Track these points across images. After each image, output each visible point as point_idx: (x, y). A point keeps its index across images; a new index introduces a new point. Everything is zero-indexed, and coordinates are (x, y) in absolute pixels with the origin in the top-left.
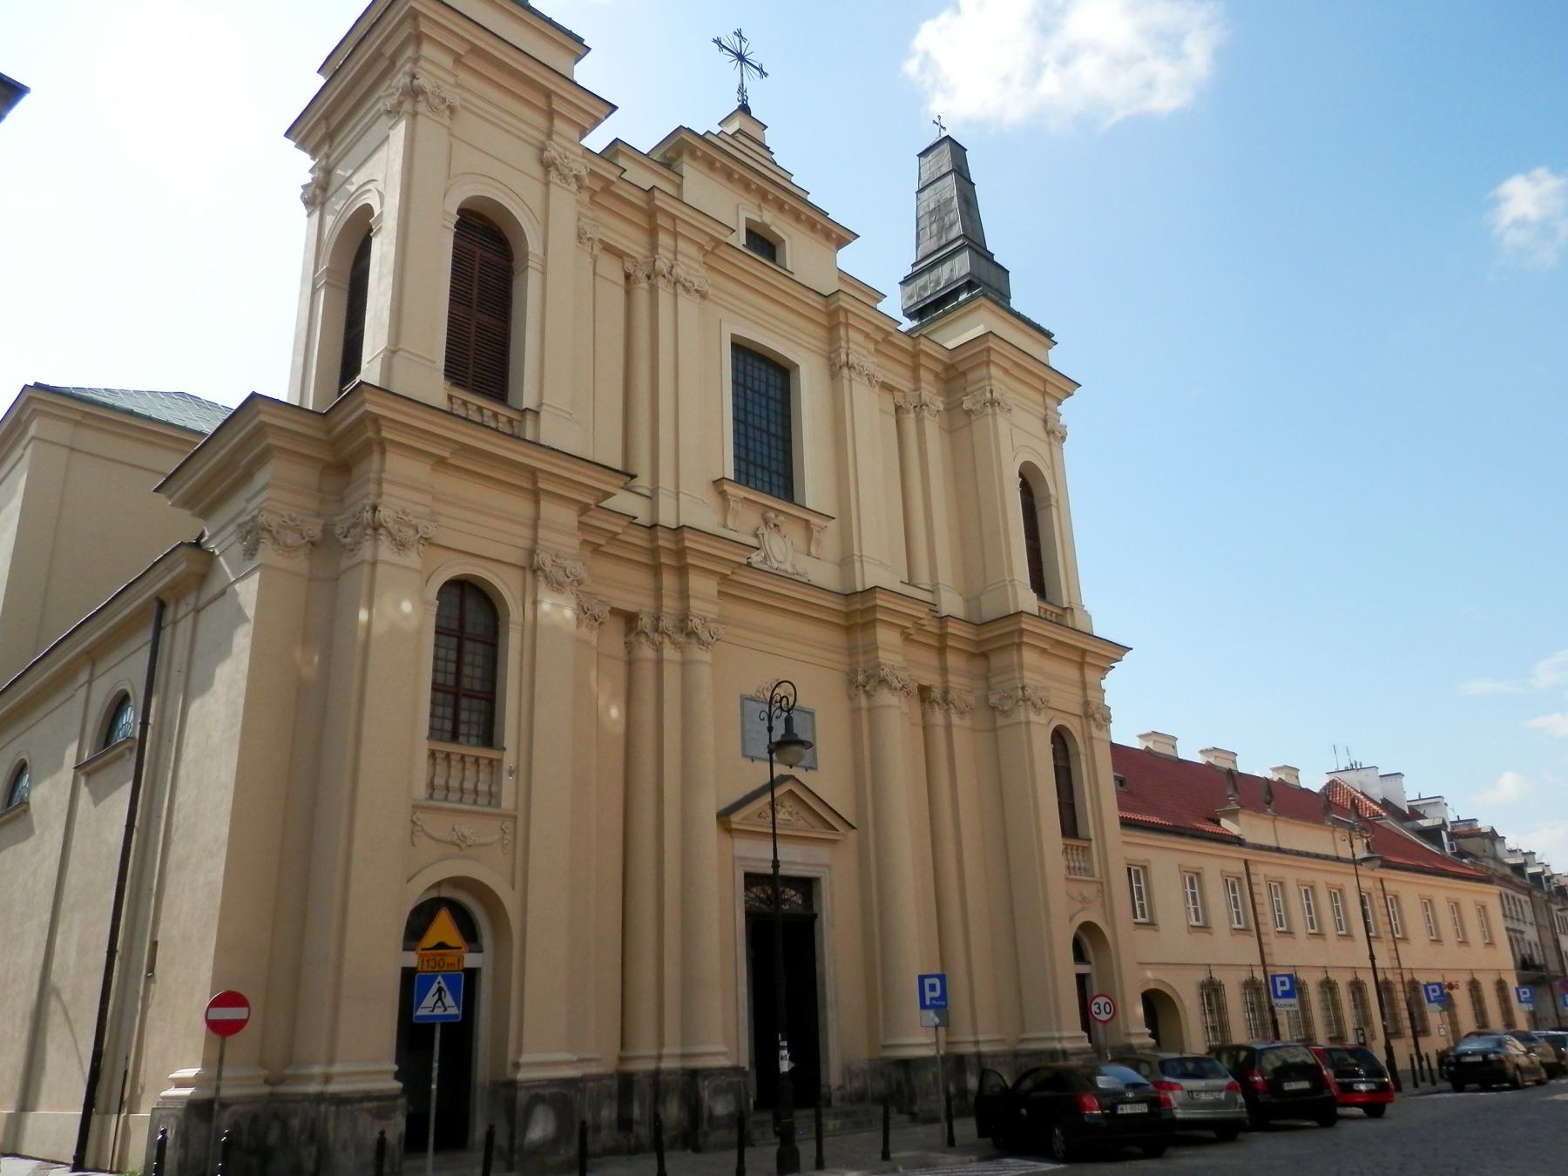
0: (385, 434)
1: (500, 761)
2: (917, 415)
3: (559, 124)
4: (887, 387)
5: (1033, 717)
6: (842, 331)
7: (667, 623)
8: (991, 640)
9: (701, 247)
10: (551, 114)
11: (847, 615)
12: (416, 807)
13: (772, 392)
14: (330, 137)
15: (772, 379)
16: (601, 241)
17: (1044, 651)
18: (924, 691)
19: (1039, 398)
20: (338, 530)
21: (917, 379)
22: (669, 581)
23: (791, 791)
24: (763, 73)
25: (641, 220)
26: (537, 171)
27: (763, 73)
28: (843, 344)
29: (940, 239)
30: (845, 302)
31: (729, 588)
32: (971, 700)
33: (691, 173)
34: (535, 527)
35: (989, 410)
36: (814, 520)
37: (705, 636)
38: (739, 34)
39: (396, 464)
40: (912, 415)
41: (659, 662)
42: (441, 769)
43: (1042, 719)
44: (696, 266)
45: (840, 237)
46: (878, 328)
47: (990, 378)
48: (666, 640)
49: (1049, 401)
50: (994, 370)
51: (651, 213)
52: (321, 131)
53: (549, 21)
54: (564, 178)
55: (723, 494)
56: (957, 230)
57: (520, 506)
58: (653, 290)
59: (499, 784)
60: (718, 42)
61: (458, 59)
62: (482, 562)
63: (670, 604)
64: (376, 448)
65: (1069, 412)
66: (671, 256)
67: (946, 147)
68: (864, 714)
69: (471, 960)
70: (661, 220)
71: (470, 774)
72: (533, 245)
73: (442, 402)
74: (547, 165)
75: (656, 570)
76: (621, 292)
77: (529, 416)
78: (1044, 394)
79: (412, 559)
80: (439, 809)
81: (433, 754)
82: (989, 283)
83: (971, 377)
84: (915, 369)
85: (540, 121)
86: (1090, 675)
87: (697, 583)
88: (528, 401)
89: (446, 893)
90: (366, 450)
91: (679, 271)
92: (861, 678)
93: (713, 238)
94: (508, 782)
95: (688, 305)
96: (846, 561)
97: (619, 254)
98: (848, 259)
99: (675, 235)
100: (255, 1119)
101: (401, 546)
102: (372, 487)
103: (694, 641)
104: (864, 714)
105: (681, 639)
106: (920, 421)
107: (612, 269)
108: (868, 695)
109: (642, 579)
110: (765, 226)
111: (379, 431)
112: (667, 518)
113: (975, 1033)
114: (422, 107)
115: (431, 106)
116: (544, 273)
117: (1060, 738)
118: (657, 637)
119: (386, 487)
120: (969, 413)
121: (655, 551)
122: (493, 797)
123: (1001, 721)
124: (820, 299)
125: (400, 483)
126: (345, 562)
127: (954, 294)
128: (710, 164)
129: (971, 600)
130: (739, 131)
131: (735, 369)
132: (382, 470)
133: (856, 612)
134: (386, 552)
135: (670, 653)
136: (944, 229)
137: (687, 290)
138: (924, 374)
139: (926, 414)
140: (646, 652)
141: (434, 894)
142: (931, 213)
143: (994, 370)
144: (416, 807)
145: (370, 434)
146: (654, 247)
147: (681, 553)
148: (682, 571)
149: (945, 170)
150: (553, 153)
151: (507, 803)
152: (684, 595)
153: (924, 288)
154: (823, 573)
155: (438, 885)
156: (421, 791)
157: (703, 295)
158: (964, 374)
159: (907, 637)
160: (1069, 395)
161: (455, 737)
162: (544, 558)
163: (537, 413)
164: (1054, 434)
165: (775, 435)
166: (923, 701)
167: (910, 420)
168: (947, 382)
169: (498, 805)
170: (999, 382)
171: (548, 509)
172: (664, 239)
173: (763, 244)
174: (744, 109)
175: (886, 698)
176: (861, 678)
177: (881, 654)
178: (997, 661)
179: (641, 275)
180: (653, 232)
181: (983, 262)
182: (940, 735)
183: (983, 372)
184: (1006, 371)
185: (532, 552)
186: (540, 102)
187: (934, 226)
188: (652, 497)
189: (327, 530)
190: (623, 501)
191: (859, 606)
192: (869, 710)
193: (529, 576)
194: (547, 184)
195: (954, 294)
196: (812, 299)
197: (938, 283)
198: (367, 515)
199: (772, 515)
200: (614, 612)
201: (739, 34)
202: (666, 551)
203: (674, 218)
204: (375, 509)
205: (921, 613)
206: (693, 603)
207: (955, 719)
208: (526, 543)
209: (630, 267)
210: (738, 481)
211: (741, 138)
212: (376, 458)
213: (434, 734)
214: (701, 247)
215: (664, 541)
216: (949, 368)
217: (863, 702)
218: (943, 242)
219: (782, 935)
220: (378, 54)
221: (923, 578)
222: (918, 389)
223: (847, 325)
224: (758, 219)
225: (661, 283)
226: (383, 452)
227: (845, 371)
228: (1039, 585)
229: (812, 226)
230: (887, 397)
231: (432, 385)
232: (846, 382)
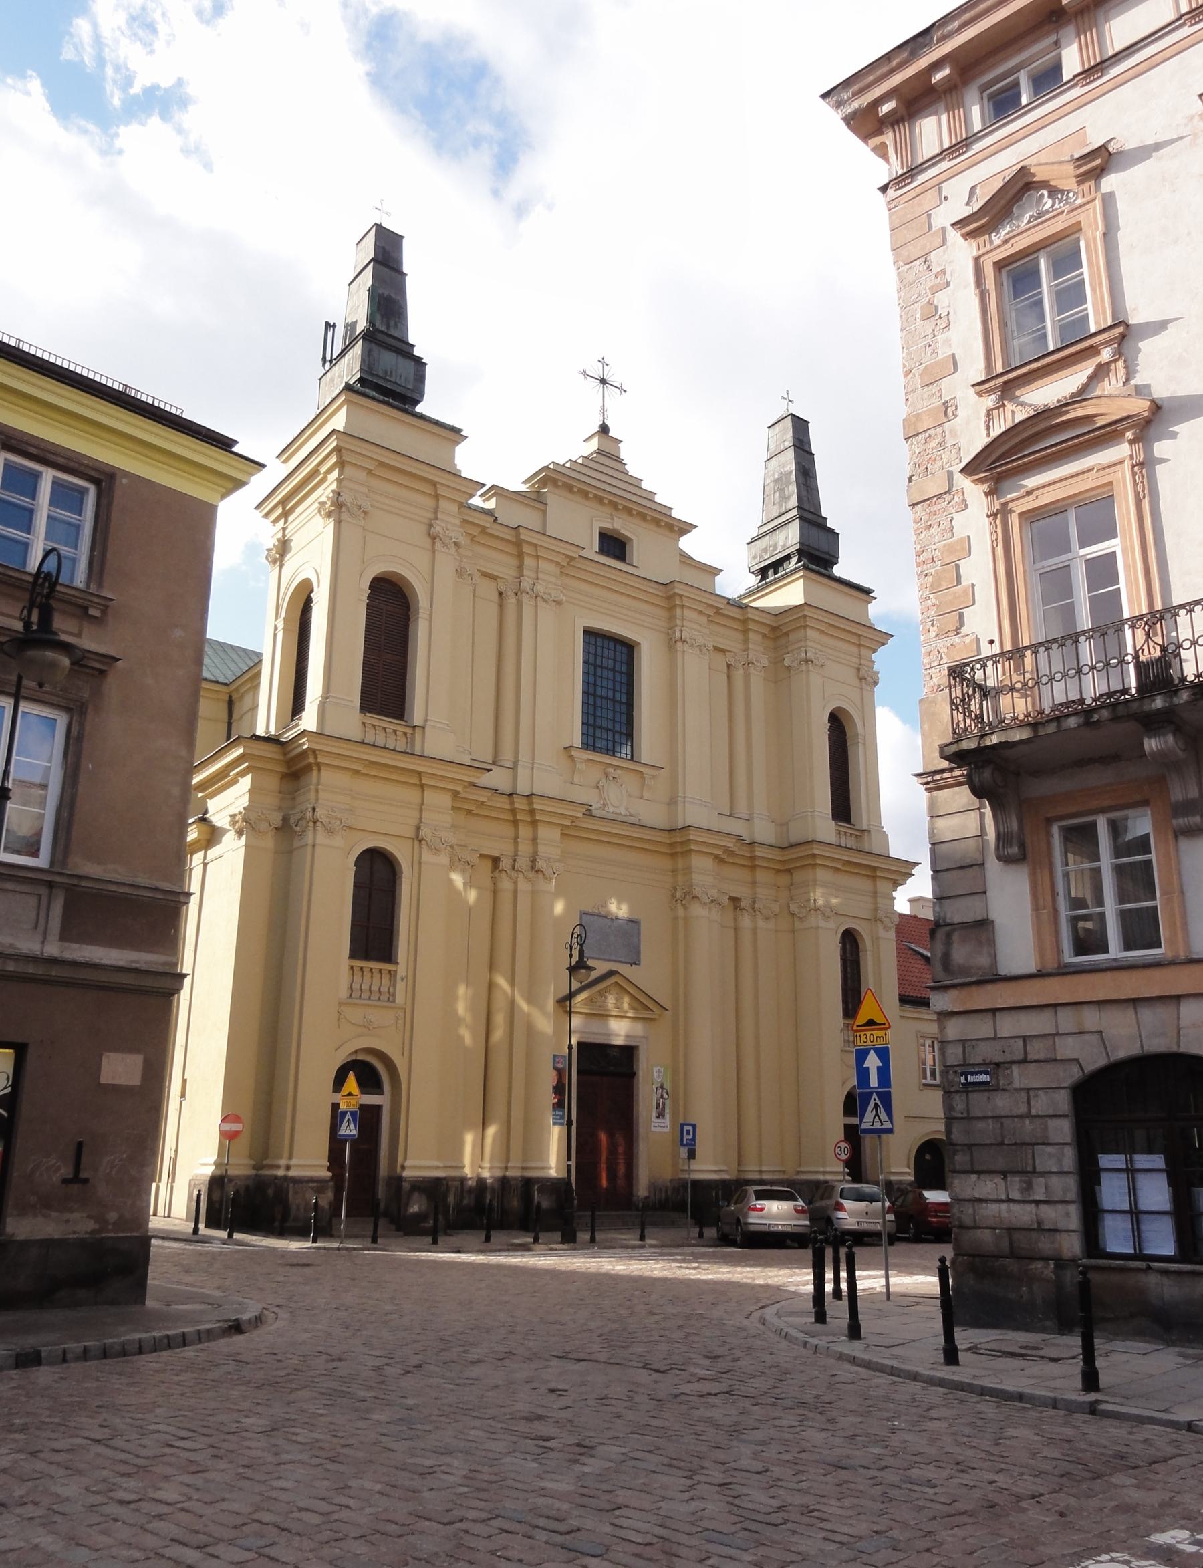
0: (320, 760)
1: (396, 972)
2: (745, 671)
3: (443, 503)
4: (716, 649)
5: (822, 923)
6: (678, 611)
7: (523, 863)
8: (794, 858)
9: (558, 564)
10: (437, 497)
11: (672, 845)
12: (341, 1003)
13: (618, 668)
14: (286, 515)
15: (618, 658)
17: (837, 869)
18: (735, 900)
19: (854, 649)
20: (292, 821)
21: (746, 641)
22: (525, 832)
23: (616, 983)
25: (511, 549)
26: (427, 542)
28: (678, 622)
29: (781, 506)
30: (678, 590)
31: (569, 832)
32: (776, 908)
33: (555, 500)
34: (421, 811)
35: (804, 668)
36: (646, 770)
37: (548, 872)
38: (602, 361)
39: (327, 776)
40: (741, 672)
41: (515, 891)
42: (357, 978)
43: (832, 925)
44: (553, 580)
45: (685, 528)
46: (709, 605)
47: (806, 639)
48: (521, 875)
49: (864, 651)
50: (810, 632)
51: (518, 543)
52: (280, 510)
53: (437, 423)
54: (445, 545)
55: (571, 757)
56: (794, 501)
57: (413, 795)
58: (519, 604)
59: (395, 986)
61: (370, 472)
62: (382, 837)
63: (524, 848)
64: (315, 768)
65: (882, 659)
66: (533, 575)
67: (788, 423)
68: (681, 922)
69: (371, 1100)
70: (526, 549)
71: (376, 980)
72: (423, 602)
73: (355, 733)
74: (434, 538)
75: (515, 823)
76: (494, 608)
77: (417, 730)
78: (860, 645)
79: (338, 841)
80: (355, 1004)
81: (352, 968)
82: (818, 553)
83: (793, 637)
84: (745, 632)
85: (430, 502)
86: (882, 886)
87: (542, 832)
88: (417, 720)
89: (360, 1057)
90: (309, 768)
91: (539, 588)
92: (679, 895)
93: (567, 556)
94: (400, 985)
95: (547, 614)
96: (673, 802)
97: (493, 578)
98: (687, 544)
99: (537, 557)
100: (247, 1188)
101: (331, 833)
102: (312, 795)
103: (541, 876)
104: (681, 922)
105: (531, 874)
106: (747, 677)
107: (488, 590)
108: (685, 908)
109: (508, 831)
110: (618, 532)
111: (316, 758)
112: (523, 788)
113: (760, 1164)
114: (344, 516)
115: (351, 514)
116: (430, 621)
117: (850, 940)
118: (514, 874)
119: (321, 795)
120: (788, 668)
121: (513, 811)
122: (392, 996)
123: (797, 925)
124: (661, 587)
125: (329, 791)
126: (297, 843)
127: (788, 558)
128: (570, 488)
129: (783, 825)
131: (586, 652)
132: (318, 783)
133: (676, 843)
134: (322, 838)
135: (523, 885)
136: (786, 498)
137: (546, 601)
138: (751, 635)
139: (752, 671)
140: (506, 884)
141: (353, 1058)
142: (775, 481)
143: (810, 633)
144: (341, 1003)
145: (311, 760)
146: (520, 567)
147: (532, 812)
148: (534, 823)
149: (787, 444)
150: (438, 528)
151: (400, 999)
152: (534, 840)
153: (765, 550)
154: (652, 814)
155: (356, 1052)
156: (344, 993)
157: (559, 603)
158: (787, 634)
159: (719, 860)
160: (883, 644)
161: (366, 957)
162: (425, 832)
163: (423, 727)
164: (867, 679)
165: (621, 703)
166: (736, 908)
167: (738, 674)
168: (775, 639)
169: (394, 1001)
170: (814, 641)
171: (430, 796)
172: (528, 562)
173: (614, 546)
174: (604, 429)
175: (697, 910)
176: (679, 895)
177: (694, 876)
178: (798, 876)
179: (510, 593)
180: (520, 556)
181: (815, 531)
182: (746, 937)
183: (801, 633)
184: (822, 632)
185: (418, 828)
186: (429, 489)
187: (777, 494)
188: (514, 769)
189: (285, 820)
190: (485, 780)
192: (686, 918)
193: (416, 843)
194: (434, 551)
195: (788, 558)
196: (652, 589)
197: (775, 548)
198: (309, 814)
199: (611, 770)
200: (482, 856)
201: (602, 361)
202: (521, 810)
203: (536, 546)
204: (314, 809)
205: (730, 843)
206: (540, 848)
207: (761, 923)
208: (415, 822)
209: (502, 588)
210: (586, 746)
212: (315, 773)
213: (353, 955)
214: (558, 564)
215: (520, 804)
216: (774, 629)
217: (681, 912)
218: (783, 510)
219: (602, 1083)
220: (315, 472)
221: (742, 810)
222: (746, 650)
223: (683, 606)
224: (609, 526)
225: (525, 599)
226: (319, 770)
227: (679, 644)
228: (842, 809)
229: (657, 522)
230: (719, 657)
231: (351, 722)
232: (679, 655)
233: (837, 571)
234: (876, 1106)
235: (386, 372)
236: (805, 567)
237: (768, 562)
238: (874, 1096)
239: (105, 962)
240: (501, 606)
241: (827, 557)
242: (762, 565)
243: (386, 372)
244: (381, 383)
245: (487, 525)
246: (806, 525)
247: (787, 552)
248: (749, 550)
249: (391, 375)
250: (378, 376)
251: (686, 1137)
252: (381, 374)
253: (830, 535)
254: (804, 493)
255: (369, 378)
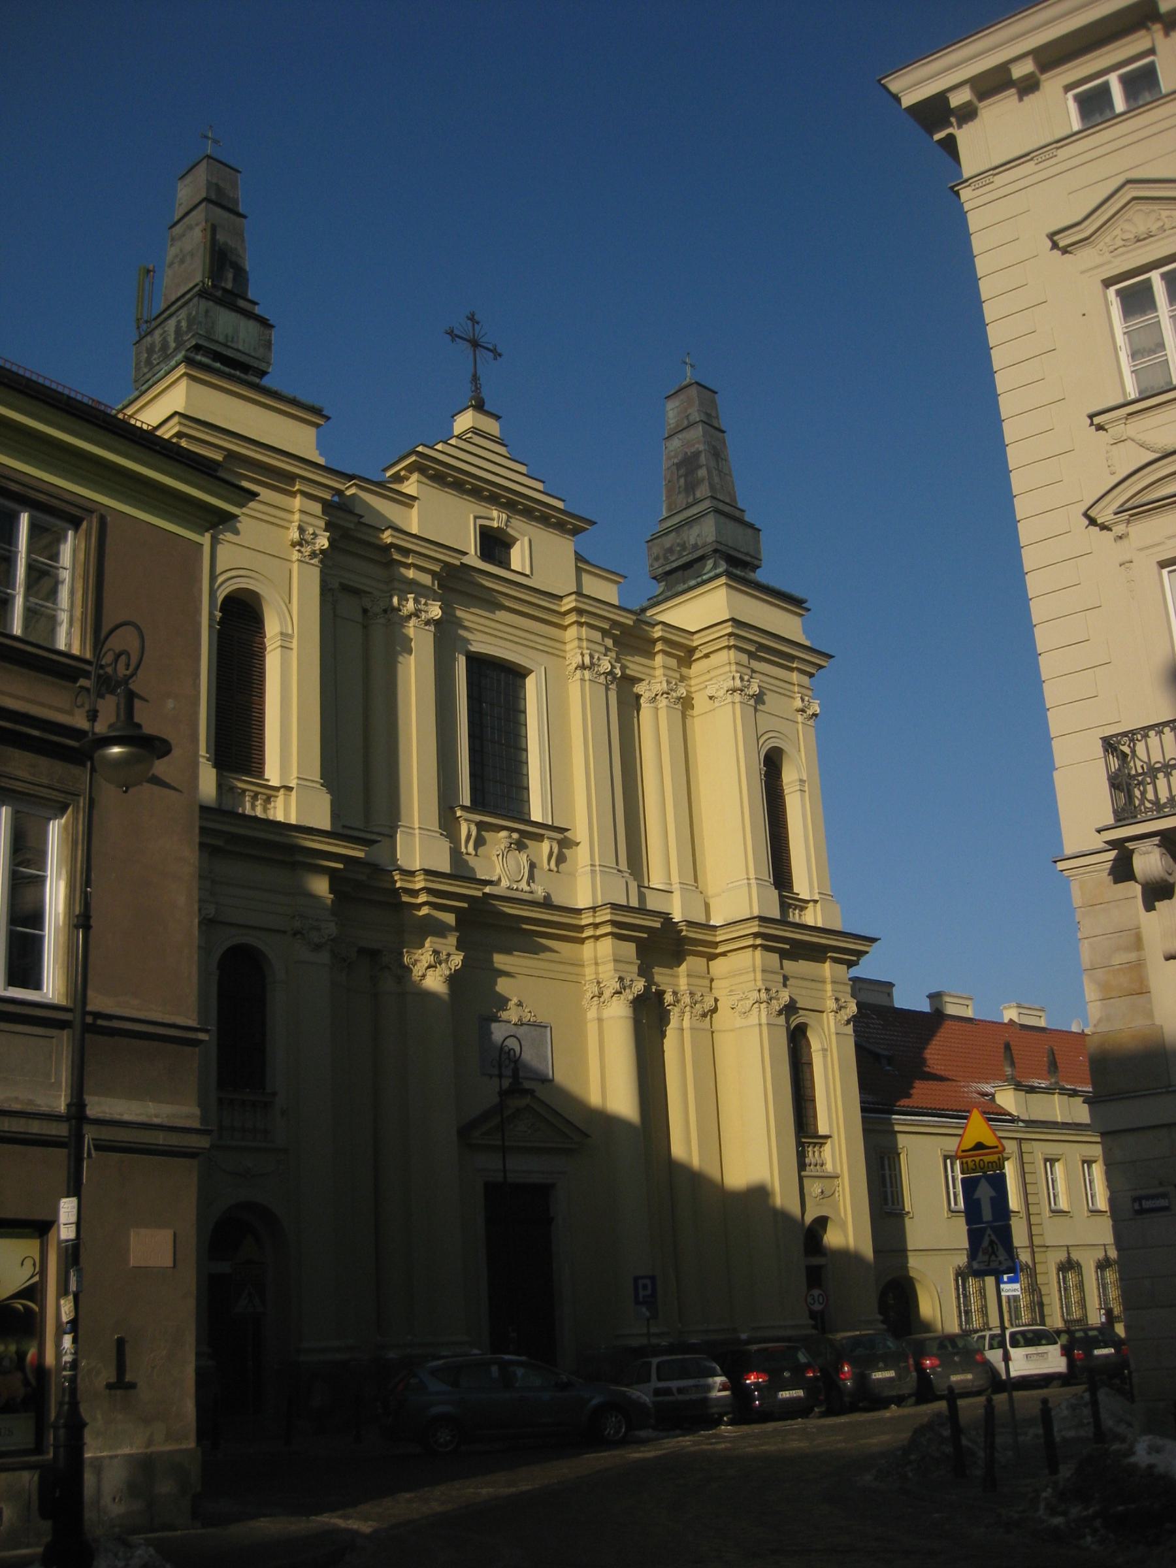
16: (341, 584)
24: (497, 354)
27: (497, 354)
38: (472, 318)
56: (703, 491)
60: (450, 333)
81: (220, 1101)
93: (446, 564)
97: (356, 592)
127: (702, 558)
130: (475, 431)
136: (690, 488)
153: (670, 550)
181: (731, 525)
187: (682, 481)
191: (590, 920)
195: (702, 558)
200: (362, 951)
201: (472, 318)
211: (477, 440)
218: (691, 499)
233: (759, 576)
234: (992, 1243)
235: (227, 336)
236: (728, 574)
237: (675, 565)
238: (989, 1231)
239: (127, 1117)
240: (365, 627)
241: (748, 559)
242: (668, 568)
243: (227, 336)
244: (220, 349)
245: (352, 526)
246: (722, 519)
247: (699, 553)
248: (649, 549)
249: (232, 341)
250: (217, 342)
251: (641, 1293)
252: (221, 339)
253: (750, 531)
254: (716, 480)
255: (206, 344)
